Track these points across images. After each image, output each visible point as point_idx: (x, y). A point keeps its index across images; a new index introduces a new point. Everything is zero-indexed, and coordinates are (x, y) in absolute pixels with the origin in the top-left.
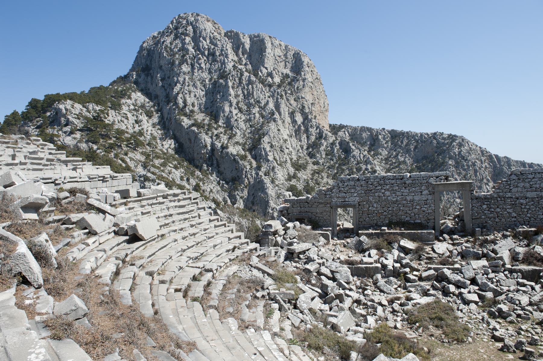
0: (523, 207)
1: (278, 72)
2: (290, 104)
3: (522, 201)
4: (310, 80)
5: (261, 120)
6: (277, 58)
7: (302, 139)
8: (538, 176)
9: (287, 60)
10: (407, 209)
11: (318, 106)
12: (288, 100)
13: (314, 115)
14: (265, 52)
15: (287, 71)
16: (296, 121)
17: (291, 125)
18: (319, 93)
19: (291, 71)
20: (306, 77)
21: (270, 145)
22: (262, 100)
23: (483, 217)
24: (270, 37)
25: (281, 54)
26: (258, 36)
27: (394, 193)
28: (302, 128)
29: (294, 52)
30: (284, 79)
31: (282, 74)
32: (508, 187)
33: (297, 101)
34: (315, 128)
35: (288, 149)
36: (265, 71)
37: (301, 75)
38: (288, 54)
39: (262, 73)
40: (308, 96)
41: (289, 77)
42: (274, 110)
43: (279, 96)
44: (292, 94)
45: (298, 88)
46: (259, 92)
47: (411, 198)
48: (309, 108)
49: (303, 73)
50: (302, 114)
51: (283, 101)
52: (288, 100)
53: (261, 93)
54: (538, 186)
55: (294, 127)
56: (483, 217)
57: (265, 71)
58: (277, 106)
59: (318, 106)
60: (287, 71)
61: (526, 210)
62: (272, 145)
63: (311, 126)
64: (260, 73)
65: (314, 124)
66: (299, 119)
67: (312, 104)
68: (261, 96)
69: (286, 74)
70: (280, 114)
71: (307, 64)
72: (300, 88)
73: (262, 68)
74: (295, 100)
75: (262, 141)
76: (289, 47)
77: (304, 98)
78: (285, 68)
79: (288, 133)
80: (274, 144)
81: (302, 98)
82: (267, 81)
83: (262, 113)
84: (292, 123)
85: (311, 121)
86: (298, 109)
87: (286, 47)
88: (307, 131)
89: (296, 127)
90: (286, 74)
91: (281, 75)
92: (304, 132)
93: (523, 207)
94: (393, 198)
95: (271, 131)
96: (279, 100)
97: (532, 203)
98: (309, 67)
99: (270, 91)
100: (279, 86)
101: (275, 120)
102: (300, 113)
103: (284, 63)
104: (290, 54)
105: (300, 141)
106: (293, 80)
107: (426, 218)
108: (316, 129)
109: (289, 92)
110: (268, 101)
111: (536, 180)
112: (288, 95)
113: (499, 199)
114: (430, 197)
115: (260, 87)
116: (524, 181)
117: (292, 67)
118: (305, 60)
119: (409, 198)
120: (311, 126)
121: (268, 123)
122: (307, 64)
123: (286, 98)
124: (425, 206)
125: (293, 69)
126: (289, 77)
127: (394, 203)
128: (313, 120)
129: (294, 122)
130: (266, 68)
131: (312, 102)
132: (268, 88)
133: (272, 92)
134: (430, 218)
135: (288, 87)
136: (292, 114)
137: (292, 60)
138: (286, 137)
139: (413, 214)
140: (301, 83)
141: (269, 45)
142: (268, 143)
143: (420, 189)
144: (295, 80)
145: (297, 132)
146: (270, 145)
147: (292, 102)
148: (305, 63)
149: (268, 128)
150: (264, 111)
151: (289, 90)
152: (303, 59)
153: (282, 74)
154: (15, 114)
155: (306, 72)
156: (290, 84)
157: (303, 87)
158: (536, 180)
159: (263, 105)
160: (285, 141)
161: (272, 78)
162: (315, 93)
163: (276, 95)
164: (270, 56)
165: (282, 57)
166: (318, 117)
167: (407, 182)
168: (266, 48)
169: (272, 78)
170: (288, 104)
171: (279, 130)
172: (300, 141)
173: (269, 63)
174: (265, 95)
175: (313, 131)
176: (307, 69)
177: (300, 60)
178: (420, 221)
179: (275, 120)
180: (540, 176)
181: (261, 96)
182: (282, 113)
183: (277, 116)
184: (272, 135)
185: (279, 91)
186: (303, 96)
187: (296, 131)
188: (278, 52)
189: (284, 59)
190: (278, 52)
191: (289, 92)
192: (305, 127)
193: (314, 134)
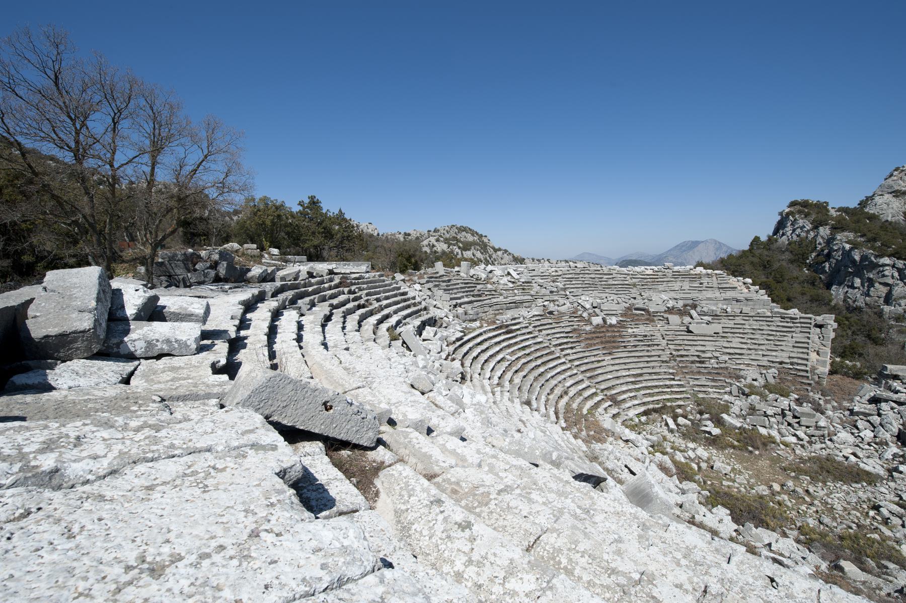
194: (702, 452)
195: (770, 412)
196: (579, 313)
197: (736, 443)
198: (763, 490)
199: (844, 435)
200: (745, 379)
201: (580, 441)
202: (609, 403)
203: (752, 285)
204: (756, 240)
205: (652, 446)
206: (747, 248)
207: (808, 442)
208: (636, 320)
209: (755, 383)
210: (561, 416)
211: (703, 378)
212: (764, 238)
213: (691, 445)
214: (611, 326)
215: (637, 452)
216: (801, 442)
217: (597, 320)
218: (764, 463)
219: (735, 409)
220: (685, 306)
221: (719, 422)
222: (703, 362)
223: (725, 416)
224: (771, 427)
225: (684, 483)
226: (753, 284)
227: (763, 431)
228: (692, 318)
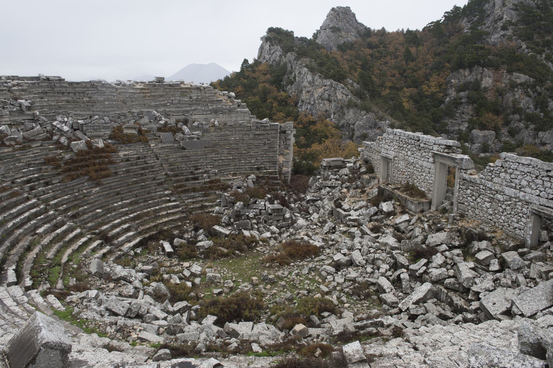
0: (500, 205)
3: (499, 196)
8: (521, 168)
23: (466, 203)
32: (490, 174)
54: (517, 181)
56: (466, 203)
61: (501, 210)
93: (500, 205)
97: (509, 203)
111: (517, 173)
113: (481, 186)
114: (433, 166)
116: (506, 172)
119: (420, 162)
154: (456, 8)
158: (517, 173)
180: (522, 170)
194: (196, 268)
195: (251, 215)
196: (55, 138)
197: (225, 251)
198: (245, 286)
199: (301, 221)
200: (232, 188)
201: (51, 298)
202: (99, 242)
203: (236, 98)
204: (246, 61)
205: (147, 277)
206: (238, 70)
207: (278, 234)
208: (128, 140)
209: (240, 191)
210: (26, 273)
211: (197, 194)
212: (251, 62)
213: (186, 264)
214: (98, 150)
215: (129, 289)
216: (273, 236)
217: (79, 145)
218: (247, 262)
219: (225, 219)
220: (178, 121)
221: (212, 234)
222: (197, 179)
223: (217, 228)
224: (252, 229)
225: (175, 305)
226: (236, 98)
227: (247, 233)
228: (184, 134)
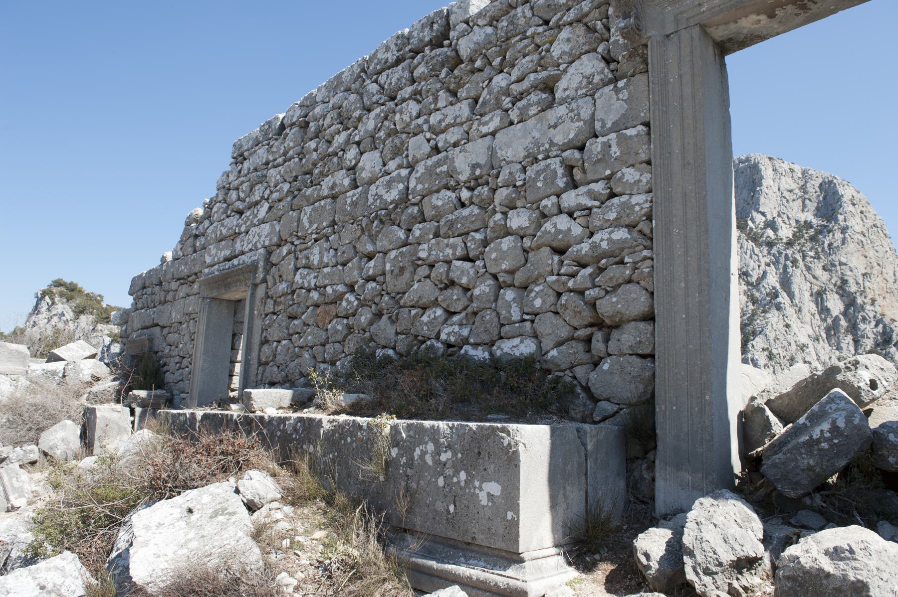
1: (788, 218)
2: (814, 277)
4: (858, 228)
5: (751, 307)
6: (786, 194)
7: (844, 345)
9: (807, 196)
10: (452, 247)
11: (880, 279)
12: (808, 269)
13: (870, 296)
14: (760, 185)
15: (809, 216)
16: (828, 310)
17: (817, 316)
18: (881, 254)
19: (815, 215)
20: (849, 224)
21: (766, 353)
22: (753, 270)
24: (770, 159)
25: (794, 186)
26: (748, 160)
27: (397, 152)
28: (843, 323)
29: (820, 181)
30: (800, 231)
31: (797, 222)
33: (831, 271)
34: (873, 323)
35: (810, 363)
36: (759, 219)
37: (836, 220)
38: (808, 185)
39: (753, 222)
40: (854, 259)
41: (812, 227)
42: (778, 286)
43: (788, 263)
44: (819, 258)
45: (830, 245)
46: (748, 257)
47: (477, 151)
48: (857, 283)
49: (841, 218)
50: (842, 296)
51: (798, 272)
52: (808, 269)
53: (751, 257)
55: (824, 320)
57: (759, 219)
58: (786, 282)
59: (880, 279)
60: (809, 216)
62: (771, 353)
63: (864, 319)
64: (750, 222)
65: (871, 315)
66: (835, 305)
67: (864, 275)
68: (752, 263)
69: (805, 222)
70: (791, 295)
71: (851, 200)
72: (835, 245)
73: (754, 214)
74: (824, 268)
75: (750, 346)
76: (810, 172)
77: (845, 264)
78: (803, 211)
79: (811, 332)
80: (775, 352)
81: (841, 264)
82: (765, 235)
83: (752, 295)
84: (820, 313)
85: (862, 308)
86: (832, 287)
87: (804, 173)
88: (853, 328)
89: (829, 321)
90: (805, 222)
91: (794, 224)
92: (847, 331)
94: (389, 186)
95: (769, 327)
96: (790, 270)
98: (854, 204)
99: (769, 253)
100: (790, 244)
101: (779, 307)
102: (837, 293)
103: (800, 201)
104: (813, 187)
105: (839, 348)
106: (819, 232)
107: (575, 310)
108: (876, 326)
109: (812, 254)
110: (765, 273)
112: (808, 259)
114: (611, 105)
115: (750, 247)
117: (817, 209)
118: (846, 193)
120: (864, 319)
121: (764, 312)
122: (851, 200)
123: (806, 266)
124: (570, 199)
125: (819, 213)
126: (812, 227)
127: (388, 216)
128: (868, 307)
129: (824, 311)
130: (763, 214)
131: (864, 271)
132: (765, 249)
133: (774, 255)
134: (608, 306)
135: (809, 245)
136: (819, 297)
137: (818, 196)
138: (804, 340)
139: (483, 288)
140: (838, 235)
141: (767, 172)
142: (764, 350)
143: (541, 65)
144: (823, 230)
145: (832, 331)
146: (766, 353)
147: (819, 272)
148: (846, 199)
149: (764, 322)
150: (758, 290)
151: (811, 249)
152: (841, 190)
153: (797, 222)
155: (848, 216)
156: (813, 239)
157: (843, 244)
159: (754, 279)
160: (803, 347)
161: (775, 230)
162: (871, 253)
163: (782, 260)
164: (770, 192)
165: (797, 191)
166: (879, 301)
167: (465, 47)
168: (762, 178)
169: (775, 230)
170: (809, 277)
171: (787, 326)
172: (839, 348)
173: (769, 204)
174: (759, 261)
175: (869, 329)
176: (851, 208)
177: (836, 193)
178: (525, 348)
179: (779, 307)
181: (752, 263)
182: (797, 293)
183: (783, 298)
184: (772, 336)
185: (789, 252)
186: (843, 260)
187: (828, 330)
188: (788, 183)
189: (800, 194)
190: (788, 183)
191: (812, 254)
192: (849, 321)
193: (871, 335)
